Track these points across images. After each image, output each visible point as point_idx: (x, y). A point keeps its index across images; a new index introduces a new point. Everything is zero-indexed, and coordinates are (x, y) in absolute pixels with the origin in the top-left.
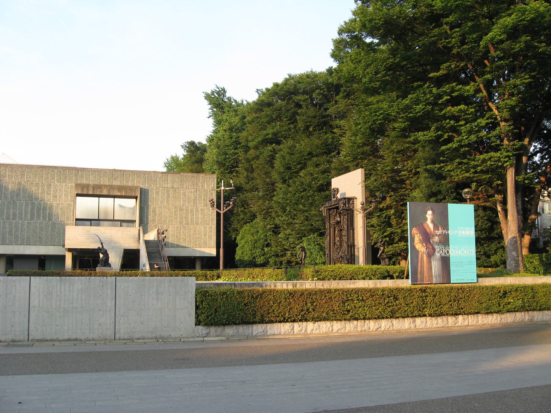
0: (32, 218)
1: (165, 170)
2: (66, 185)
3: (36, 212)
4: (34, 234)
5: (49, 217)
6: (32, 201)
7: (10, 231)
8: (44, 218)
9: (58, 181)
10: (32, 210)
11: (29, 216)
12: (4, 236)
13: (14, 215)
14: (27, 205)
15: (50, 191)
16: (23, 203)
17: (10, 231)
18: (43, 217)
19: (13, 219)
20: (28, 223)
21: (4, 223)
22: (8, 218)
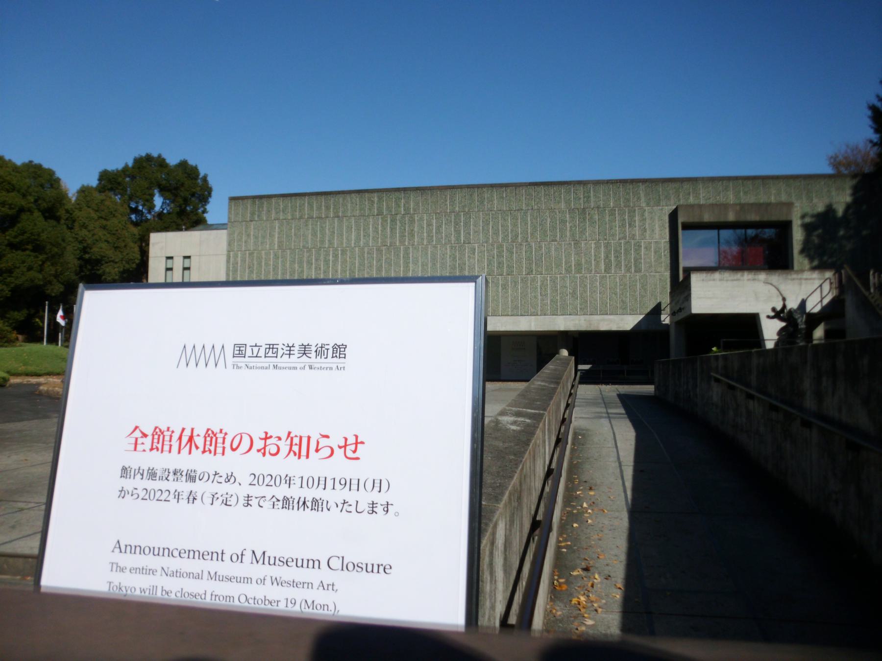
0: (608, 269)
1: (829, 170)
2: (662, 209)
3: (613, 259)
4: (614, 295)
5: (636, 266)
6: (606, 239)
7: (574, 294)
8: (628, 270)
9: (648, 205)
10: (607, 257)
11: (603, 267)
12: (565, 301)
13: (579, 265)
14: (598, 247)
15: (635, 221)
16: (591, 243)
17: (574, 294)
18: (626, 266)
19: (579, 271)
20: (602, 278)
21: (563, 279)
22: (568, 270)
